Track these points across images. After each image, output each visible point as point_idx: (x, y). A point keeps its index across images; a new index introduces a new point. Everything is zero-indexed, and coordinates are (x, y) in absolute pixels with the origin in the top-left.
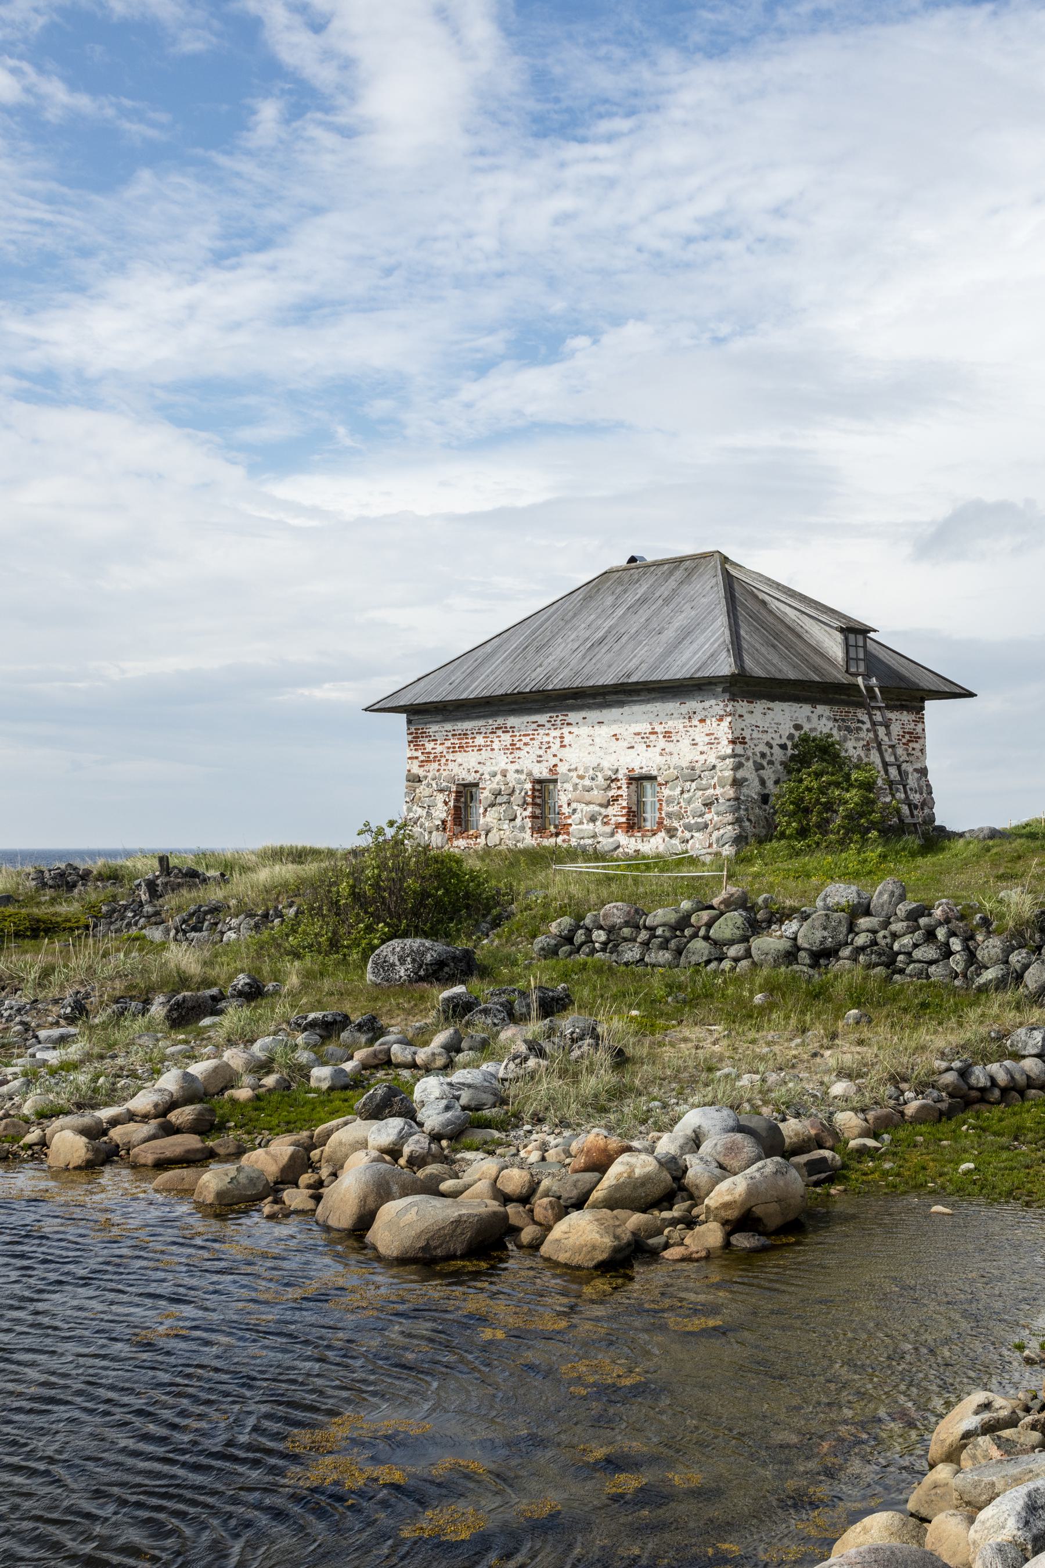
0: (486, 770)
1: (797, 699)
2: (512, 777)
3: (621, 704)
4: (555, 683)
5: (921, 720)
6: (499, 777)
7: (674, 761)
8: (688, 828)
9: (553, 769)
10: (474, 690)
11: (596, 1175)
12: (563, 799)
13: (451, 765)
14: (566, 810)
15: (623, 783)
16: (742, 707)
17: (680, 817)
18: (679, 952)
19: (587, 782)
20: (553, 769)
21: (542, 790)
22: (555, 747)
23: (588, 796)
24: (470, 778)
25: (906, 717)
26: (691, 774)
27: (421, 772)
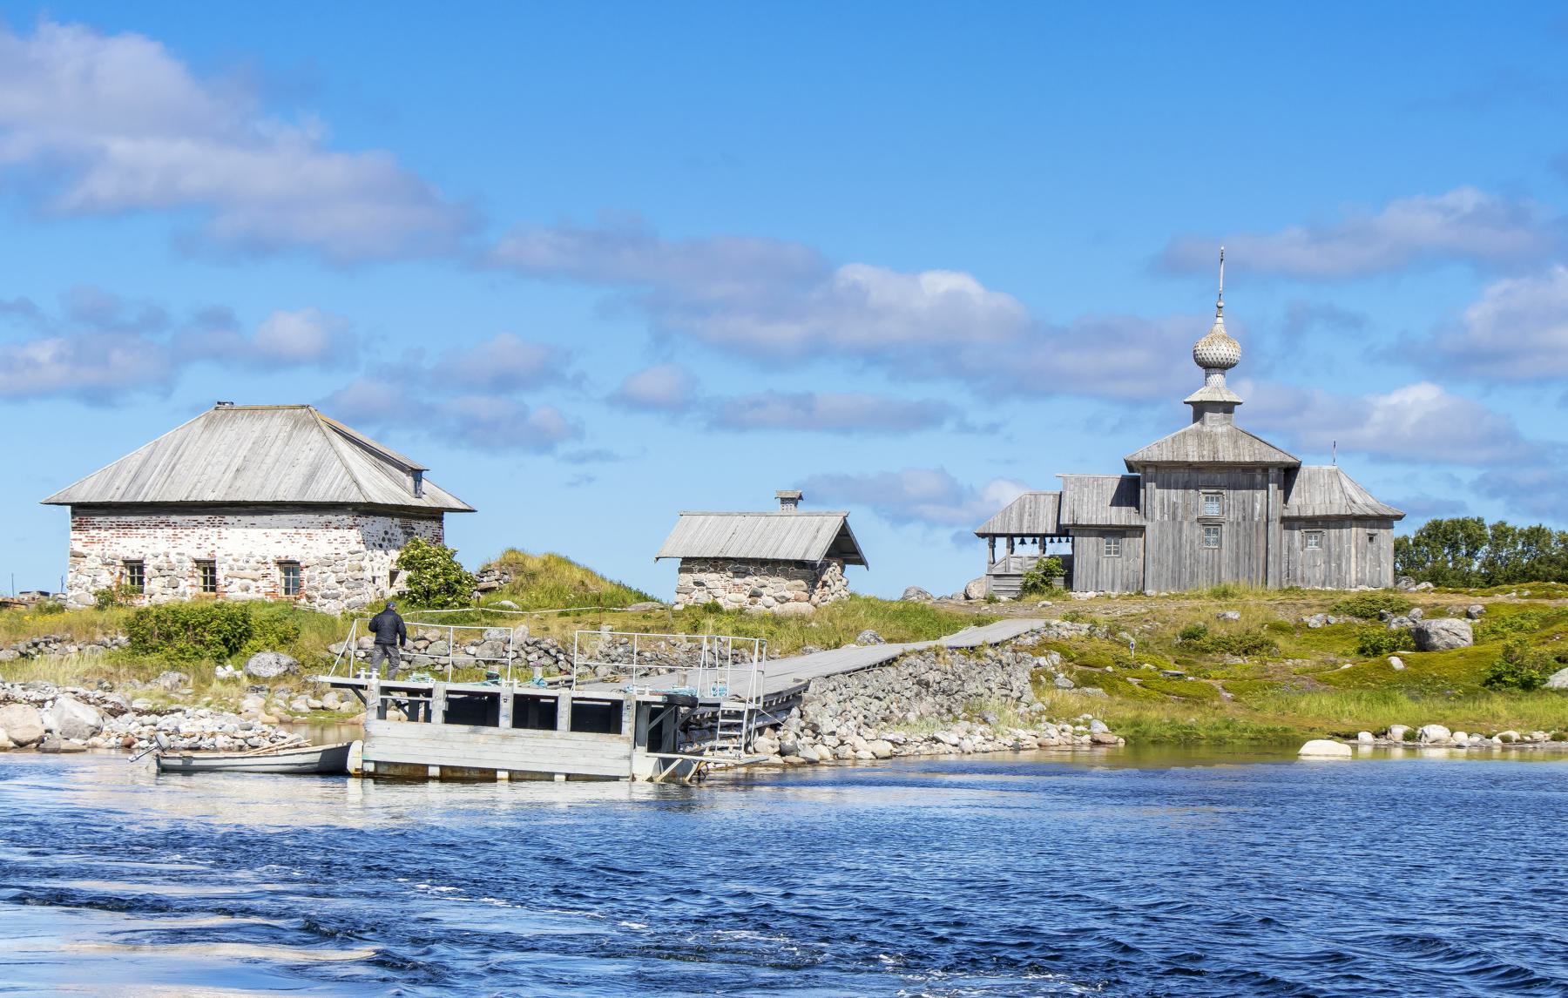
0: (148, 552)
2: (174, 559)
3: (270, 513)
5: (441, 527)
6: (161, 558)
7: (313, 553)
13: (115, 547)
15: (272, 565)
17: (317, 589)
19: (241, 564)
22: (214, 539)
26: (327, 563)
27: (85, 551)
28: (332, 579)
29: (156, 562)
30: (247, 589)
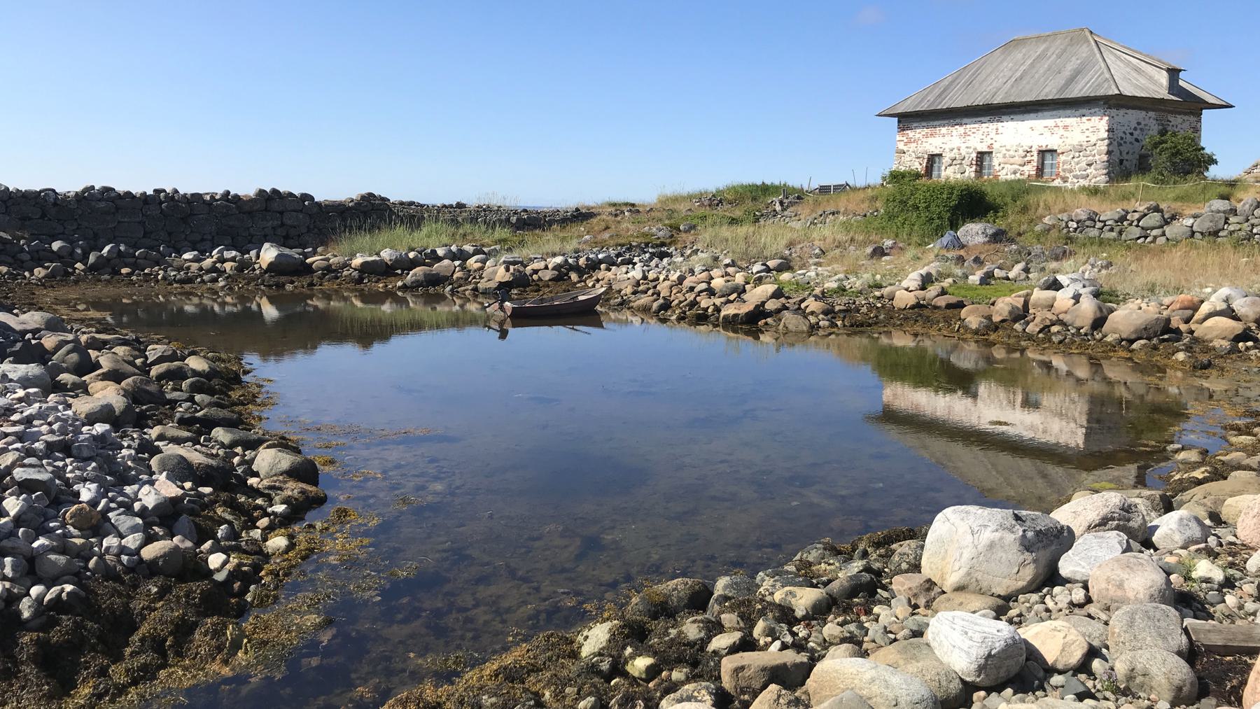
0: (947, 147)
1: (1140, 109)
3: (1036, 111)
4: (998, 100)
7: (1069, 141)
8: (1076, 177)
9: (990, 146)
10: (944, 105)
11: (1190, 312)
12: (995, 162)
14: (997, 168)
15: (1035, 154)
16: (1114, 112)
18: (1120, 233)
19: (1012, 153)
20: (990, 146)
21: (982, 157)
22: (993, 135)
23: (1012, 160)
24: (937, 152)
25: (1192, 118)
26: (1080, 149)
27: (905, 149)
28: (1083, 165)
29: (952, 155)
30: (1015, 173)
